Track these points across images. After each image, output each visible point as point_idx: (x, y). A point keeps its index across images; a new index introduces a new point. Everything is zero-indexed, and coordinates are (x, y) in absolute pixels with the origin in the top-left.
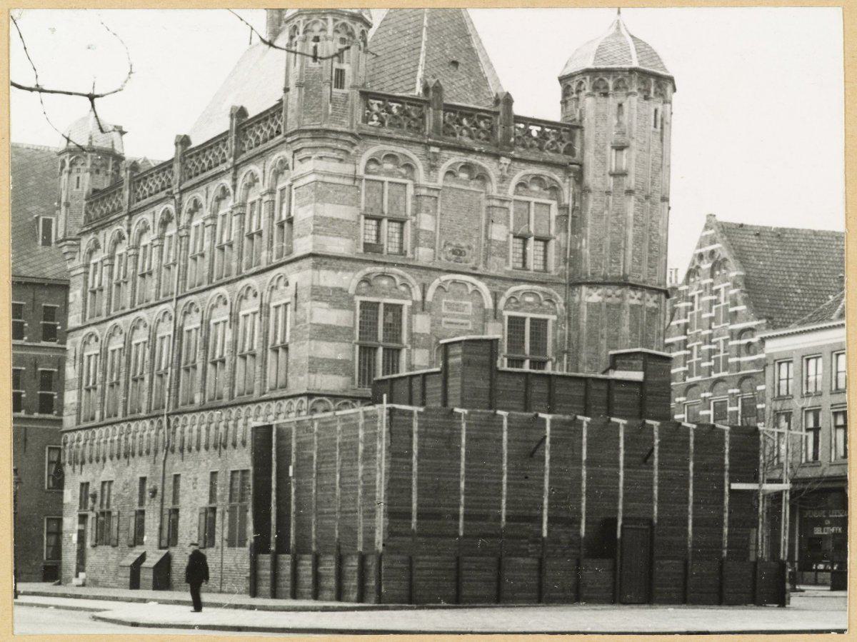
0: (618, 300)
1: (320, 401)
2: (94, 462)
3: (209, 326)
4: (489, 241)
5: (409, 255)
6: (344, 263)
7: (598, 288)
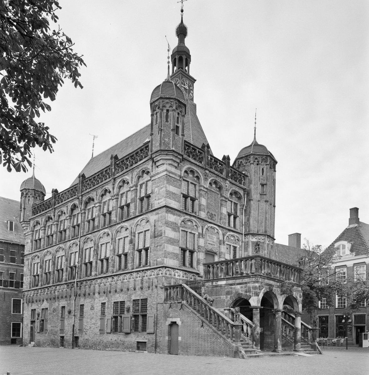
1: (168, 270)
2: (41, 301)
3: (98, 245)
5: (197, 214)
7: (256, 236)
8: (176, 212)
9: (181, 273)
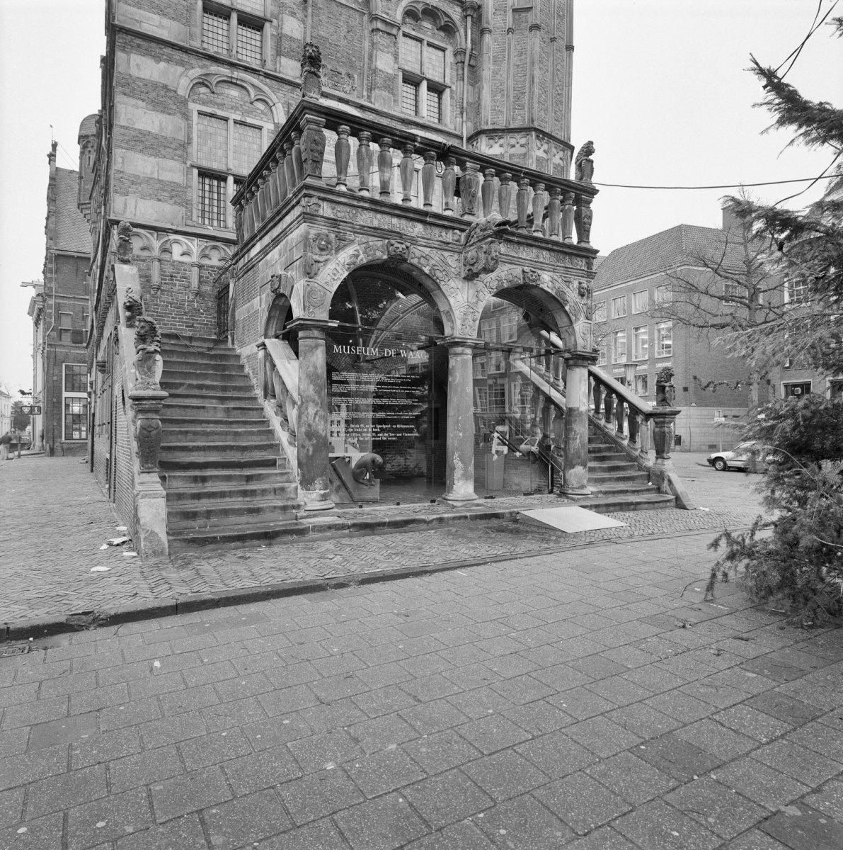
0: (523, 150)
4: (374, 71)
6: (168, 50)
8: (165, 50)
9: (195, 246)
